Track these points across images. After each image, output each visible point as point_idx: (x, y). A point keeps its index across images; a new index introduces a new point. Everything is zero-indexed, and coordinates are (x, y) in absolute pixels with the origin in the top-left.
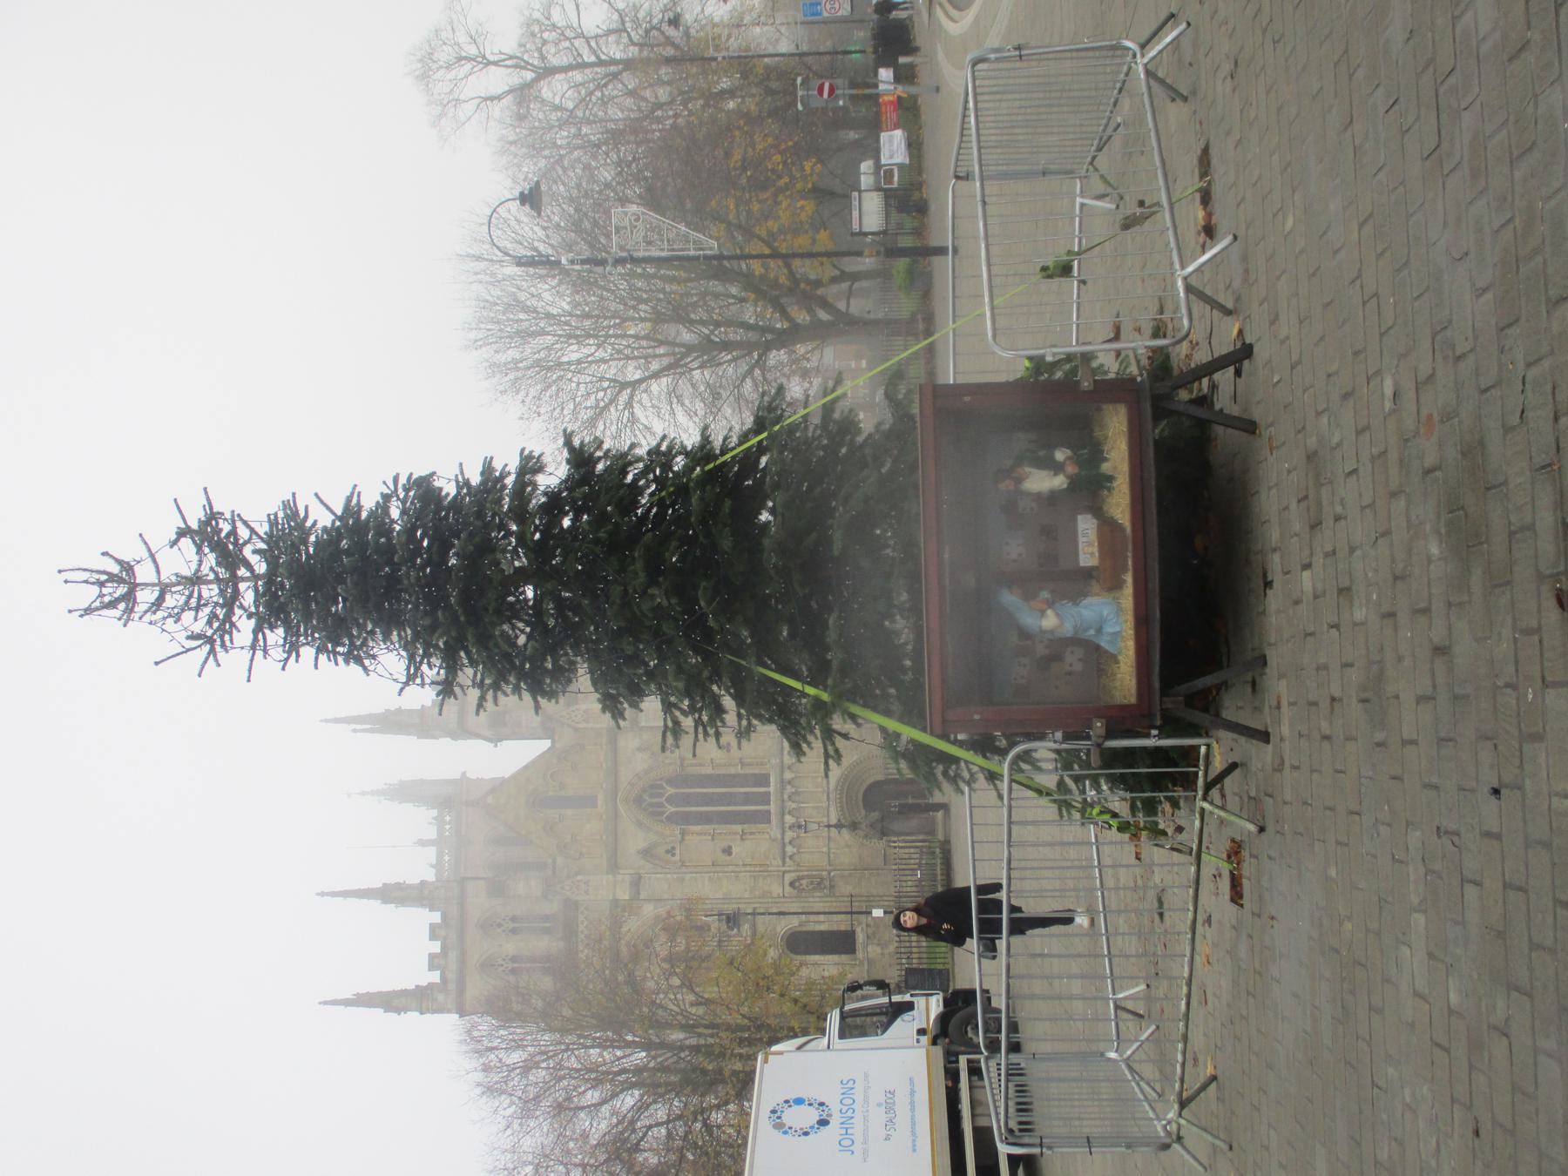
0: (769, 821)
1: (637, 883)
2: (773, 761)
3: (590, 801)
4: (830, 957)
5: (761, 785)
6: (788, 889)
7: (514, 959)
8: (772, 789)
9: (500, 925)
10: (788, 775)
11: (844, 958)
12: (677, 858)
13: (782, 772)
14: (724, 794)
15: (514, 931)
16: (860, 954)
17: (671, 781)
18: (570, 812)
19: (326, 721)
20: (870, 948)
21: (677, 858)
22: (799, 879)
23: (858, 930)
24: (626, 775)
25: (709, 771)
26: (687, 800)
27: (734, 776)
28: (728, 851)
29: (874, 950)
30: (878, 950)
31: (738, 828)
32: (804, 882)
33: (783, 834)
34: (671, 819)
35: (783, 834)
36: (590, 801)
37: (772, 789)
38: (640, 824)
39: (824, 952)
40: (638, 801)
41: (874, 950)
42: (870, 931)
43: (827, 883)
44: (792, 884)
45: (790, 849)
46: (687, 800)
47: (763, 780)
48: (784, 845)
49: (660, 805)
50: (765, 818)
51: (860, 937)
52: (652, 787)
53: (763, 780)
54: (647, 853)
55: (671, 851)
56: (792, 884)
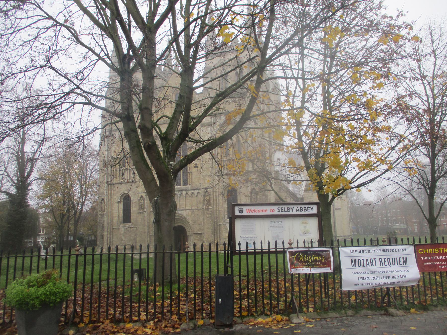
2: (190, 186)
5: (183, 182)
6: (140, 195)
8: (182, 186)
10: (184, 193)
11: (121, 219)
13: (185, 190)
16: (123, 225)
23: (130, 224)
29: (122, 230)
30: (122, 233)
37: (182, 186)
39: (124, 210)
41: (122, 230)
42: (129, 229)
43: (142, 211)
44: (142, 196)
51: (127, 225)
56: (142, 196)
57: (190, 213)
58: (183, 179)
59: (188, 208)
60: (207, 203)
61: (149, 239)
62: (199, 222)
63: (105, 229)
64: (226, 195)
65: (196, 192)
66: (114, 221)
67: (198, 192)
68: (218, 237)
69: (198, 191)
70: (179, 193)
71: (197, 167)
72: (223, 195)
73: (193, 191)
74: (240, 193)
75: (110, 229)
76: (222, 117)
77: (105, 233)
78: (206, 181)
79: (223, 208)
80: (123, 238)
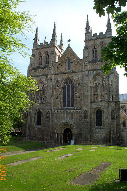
0: (63, 107)
1: (51, 79)
2: (75, 107)
3: (69, 69)
4: (36, 120)
6: (47, 111)
7: (42, 58)
8: (70, 107)
9: (47, 55)
10: (72, 111)
12: (56, 87)
14: (70, 97)
15: (46, 58)
16: (36, 126)
17: (73, 85)
18: (67, 65)
19: (87, 16)
20: (37, 128)
21: (56, 87)
22: (49, 113)
23: (41, 126)
24: (73, 75)
25: (74, 93)
26: (69, 89)
27: (73, 99)
28: (57, 98)
29: (36, 129)
31: (62, 100)
32: (49, 114)
33: (60, 110)
34: (65, 86)
35: (60, 110)
36: (69, 69)
37: (70, 107)
38: (63, 79)
40: (69, 79)
41: (36, 129)
45: (56, 111)
46: (69, 89)
47: (72, 106)
48: (57, 110)
49: (68, 83)
50: (64, 106)
51: (39, 126)
52: (72, 81)
53: (72, 106)
54: (57, 80)
55: (58, 86)
57: (75, 122)
58: (71, 104)
59: (73, 119)
60: (86, 117)
61: (51, 135)
62: (80, 127)
63: (27, 128)
64: (95, 113)
65: (79, 111)
66: (32, 124)
67: (80, 111)
68: (91, 136)
69: (80, 110)
70: (69, 111)
71: (80, 97)
72: (94, 113)
73: (77, 110)
74: (104, 113)
75: (30, 128)
76: (94, 71)
77: (27, 130)
78: (86, 105)
79: (94, 120)
80: (36, 133)
